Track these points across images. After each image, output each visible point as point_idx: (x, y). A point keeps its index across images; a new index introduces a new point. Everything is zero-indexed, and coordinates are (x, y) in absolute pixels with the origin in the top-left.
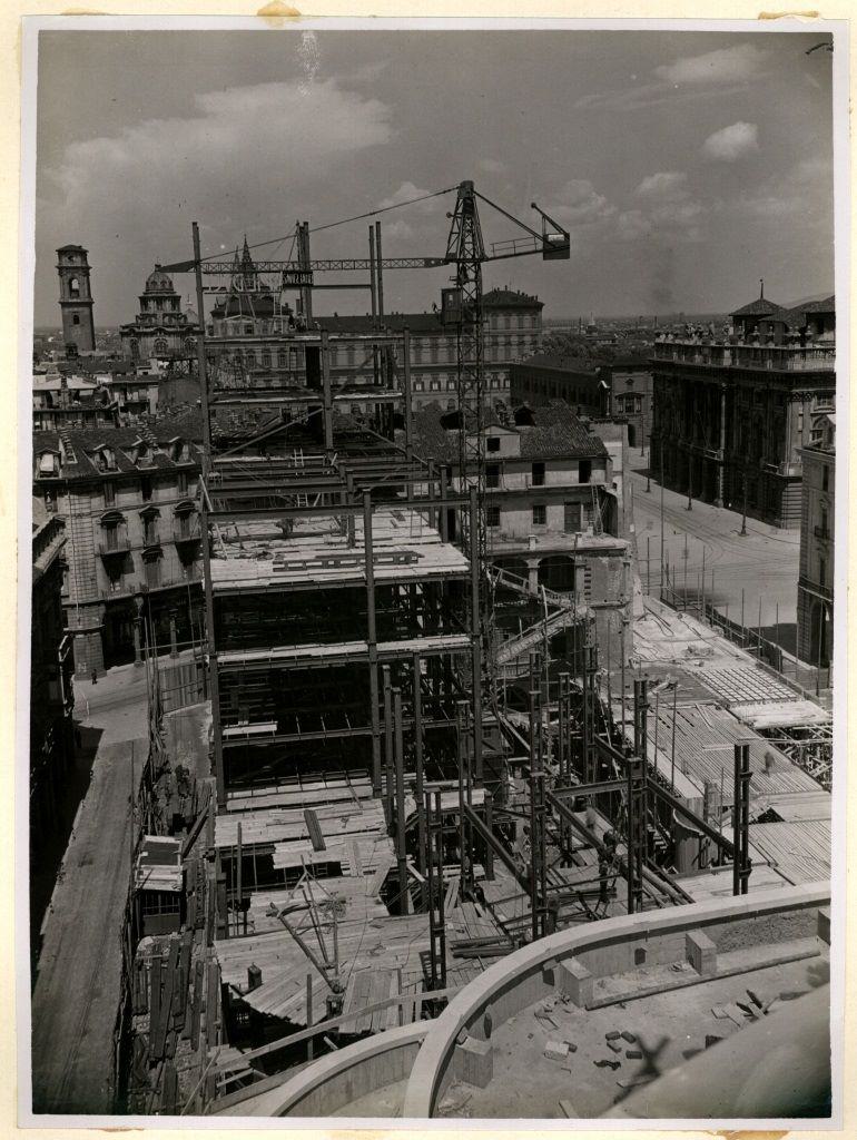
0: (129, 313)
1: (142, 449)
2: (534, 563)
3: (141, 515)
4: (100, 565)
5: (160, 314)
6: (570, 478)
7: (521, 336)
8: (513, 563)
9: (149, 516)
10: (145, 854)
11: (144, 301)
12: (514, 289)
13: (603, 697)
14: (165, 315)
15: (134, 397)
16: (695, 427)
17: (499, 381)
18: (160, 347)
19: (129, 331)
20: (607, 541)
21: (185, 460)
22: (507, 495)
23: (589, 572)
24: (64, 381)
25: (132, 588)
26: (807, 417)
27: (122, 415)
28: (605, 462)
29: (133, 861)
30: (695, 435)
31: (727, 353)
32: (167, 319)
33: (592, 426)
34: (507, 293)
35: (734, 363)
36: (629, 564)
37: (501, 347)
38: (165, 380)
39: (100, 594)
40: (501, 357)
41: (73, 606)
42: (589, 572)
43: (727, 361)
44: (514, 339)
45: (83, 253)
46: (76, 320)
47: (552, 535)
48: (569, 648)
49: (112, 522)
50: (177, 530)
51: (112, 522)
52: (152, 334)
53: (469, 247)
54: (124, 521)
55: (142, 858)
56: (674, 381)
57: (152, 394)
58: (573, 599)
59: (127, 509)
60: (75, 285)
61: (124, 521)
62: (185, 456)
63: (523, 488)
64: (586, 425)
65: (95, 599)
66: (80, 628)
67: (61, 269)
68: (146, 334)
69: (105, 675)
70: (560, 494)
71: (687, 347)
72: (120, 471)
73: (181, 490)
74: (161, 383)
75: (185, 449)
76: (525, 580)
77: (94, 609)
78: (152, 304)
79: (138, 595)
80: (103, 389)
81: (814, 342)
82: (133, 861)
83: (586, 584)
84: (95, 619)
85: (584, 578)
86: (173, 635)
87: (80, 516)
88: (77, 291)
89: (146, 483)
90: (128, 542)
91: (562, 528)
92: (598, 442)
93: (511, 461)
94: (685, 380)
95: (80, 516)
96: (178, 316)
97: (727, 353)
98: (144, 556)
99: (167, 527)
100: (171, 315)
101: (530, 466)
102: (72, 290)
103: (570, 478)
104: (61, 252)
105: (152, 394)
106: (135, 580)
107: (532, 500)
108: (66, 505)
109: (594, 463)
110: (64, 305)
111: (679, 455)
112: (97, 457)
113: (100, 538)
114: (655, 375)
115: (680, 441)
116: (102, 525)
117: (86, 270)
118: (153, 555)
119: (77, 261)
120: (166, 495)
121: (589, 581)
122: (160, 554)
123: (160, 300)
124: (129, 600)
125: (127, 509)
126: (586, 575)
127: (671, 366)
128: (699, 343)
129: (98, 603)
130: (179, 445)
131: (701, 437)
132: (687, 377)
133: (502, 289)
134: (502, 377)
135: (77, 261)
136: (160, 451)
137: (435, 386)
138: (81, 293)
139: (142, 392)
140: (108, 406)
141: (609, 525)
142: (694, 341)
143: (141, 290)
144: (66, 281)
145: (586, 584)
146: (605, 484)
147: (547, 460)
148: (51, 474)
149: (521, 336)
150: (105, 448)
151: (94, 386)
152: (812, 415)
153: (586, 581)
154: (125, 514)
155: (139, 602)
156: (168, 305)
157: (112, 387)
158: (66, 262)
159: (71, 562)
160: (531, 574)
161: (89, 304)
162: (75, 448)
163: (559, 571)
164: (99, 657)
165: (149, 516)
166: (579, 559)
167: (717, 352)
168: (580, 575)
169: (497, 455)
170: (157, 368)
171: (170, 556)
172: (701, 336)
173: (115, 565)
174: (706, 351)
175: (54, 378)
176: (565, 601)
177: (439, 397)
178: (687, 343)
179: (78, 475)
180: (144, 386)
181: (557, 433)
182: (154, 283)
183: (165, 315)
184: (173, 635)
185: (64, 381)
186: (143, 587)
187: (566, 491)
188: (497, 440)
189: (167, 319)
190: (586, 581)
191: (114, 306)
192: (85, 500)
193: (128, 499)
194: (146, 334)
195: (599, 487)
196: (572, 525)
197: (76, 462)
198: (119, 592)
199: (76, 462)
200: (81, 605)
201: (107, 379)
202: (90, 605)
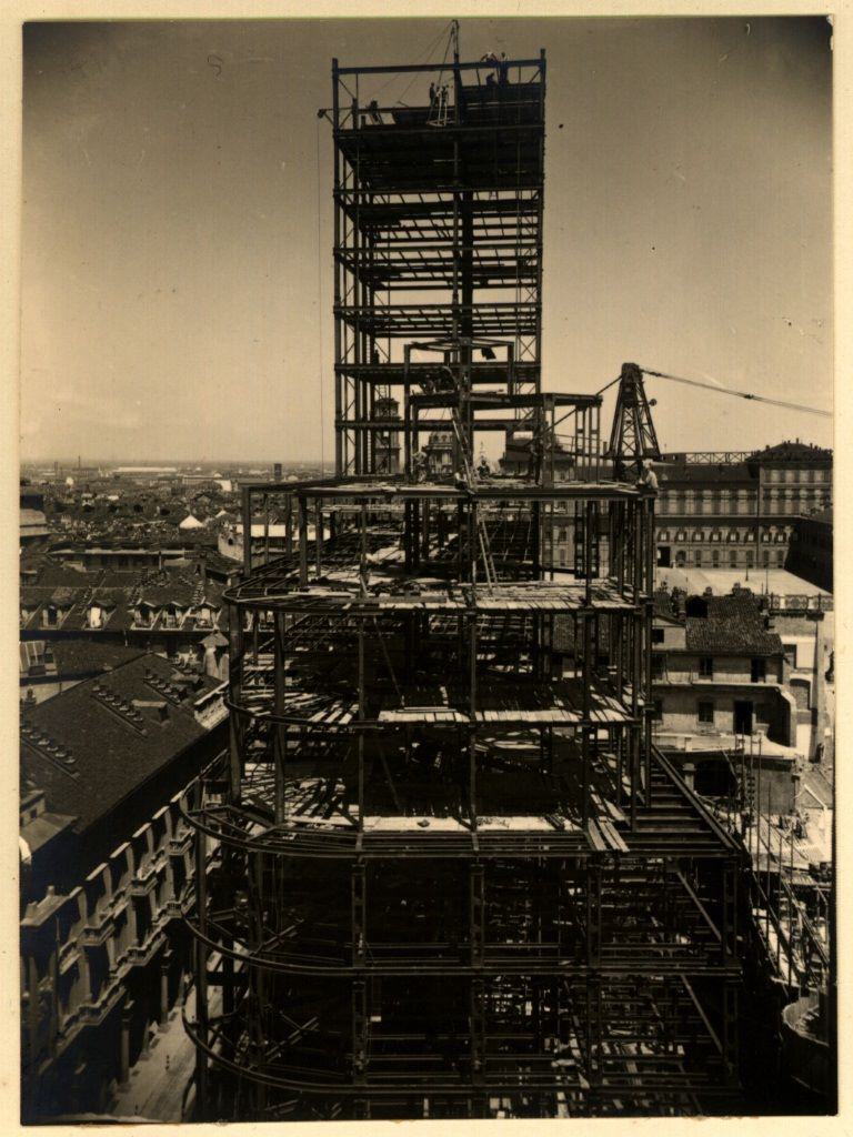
5: (439, 466)
6: (742, 679)
7: (811, 490)
12: (806, 442)
17: (770, 534)
20: (772, 749)
22: (670, 689)
28: (781, 664)
33: (771, 622)
34: (799, 446)
36: (798, 778)
37: (788, 501)
40: (788, 510)
44: (803, 493)
47: (720, 736)
53: (629, 440)
63: (686, 683)
64: (766, 620)
70: (724, 692)
91: (731, 729)
92: (776, 638)
93: (675, 653)
101: (695, 662)
103: (742, 679)
109: (769, 665)
133: (793, 441)
134: (788, 531)
137: (715, 537)
141: (782, 735)
146: (780, 686)
149: (811, 490)
163: (718, 774)
169: (660, 646)
177: (720, 549)
181: (732, 628)
183: (444, 466)
195: (773, 689)
196: (742, 726)
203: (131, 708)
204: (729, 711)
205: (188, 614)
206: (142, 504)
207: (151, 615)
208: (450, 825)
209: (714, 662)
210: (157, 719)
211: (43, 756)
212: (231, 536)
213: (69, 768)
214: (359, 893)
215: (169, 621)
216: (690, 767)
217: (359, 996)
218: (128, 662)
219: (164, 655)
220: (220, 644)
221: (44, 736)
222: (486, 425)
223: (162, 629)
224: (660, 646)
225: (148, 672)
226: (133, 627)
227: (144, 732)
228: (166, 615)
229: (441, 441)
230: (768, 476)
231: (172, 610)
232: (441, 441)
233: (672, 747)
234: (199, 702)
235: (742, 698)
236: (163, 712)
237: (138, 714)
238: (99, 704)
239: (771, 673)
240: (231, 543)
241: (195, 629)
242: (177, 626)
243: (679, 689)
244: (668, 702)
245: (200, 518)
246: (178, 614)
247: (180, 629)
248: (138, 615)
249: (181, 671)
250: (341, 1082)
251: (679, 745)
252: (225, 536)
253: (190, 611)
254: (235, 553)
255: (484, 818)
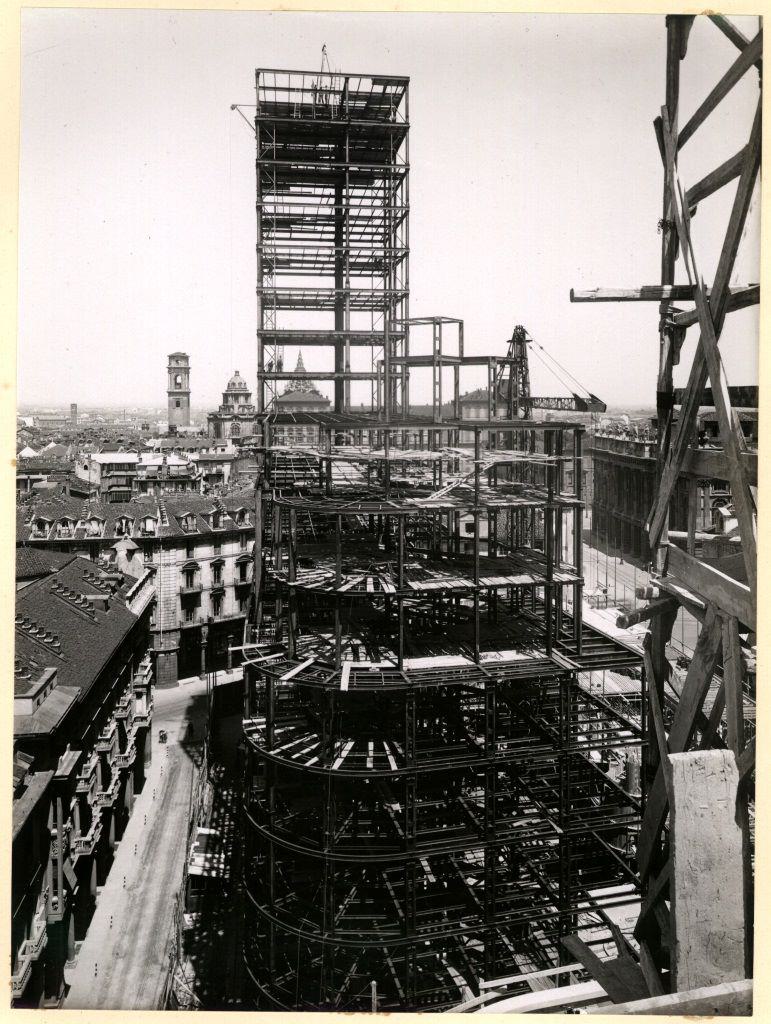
0: (215, 403)
1: (217, 515)
3: (211, 565)
4: (179, 602)
5: (236, 406)
9: (217, 566)
10: (197, 844)
11: (226, 396)
14: (240, 406)
15: (214, 471)
16: (625, 500)
18: (235, 430)
19: (215, 419)
21: (247, 525)
24: (165, 459)
25: (201, 620)
26: (707, 498)
27: (203, 483)
29: (188, 850)
30: (625, 505)
31: (647, 449)
32: (241, 409)
35: (651, 455)
38: (236, 459)
39: (178, 624)
41: (158, 633)
43: (647, 455)
45: (185, 358)
46: (178, 404)
49: (190, 571)
50: (238, 577)
51: (190, 571)
52: (230, 420)
54: (198, 569)
55: (195, 847)
56: (610, 464)
57: (226, 469)
59: (203, 560)
60: (179, 380)
61: (198, 569)
62: (247, 522)
65: (173, 627)
66: (162, 649)
67: (170, 369)
68: (225, 420)
69: (178, 685)
71: (618, 441)
72: (199, 532)
73: (242, 546)
74: (233, 461)
75: (247, 516)
77: (173, 634)
78: (230, 399)
79: (205, 625)
80: (192, 465)
81: (710, 443)
82: (188, 850)
84: (173, 643)
86: (230, 658)
87: (168, 565)
88: (180, 384)
89: (216, 540)
90: (201, 586)
94: (616, 466)
95: (168, 565)
96: (249, 407)
97: (647, 449)
98: (211, 595)
99: (230, 574)
100: (244, 407)
102: (176, 384)
104: (171, 357)
105: (226, 469)
106: (204, 610)
108: (160, 557)
110: (170, 394)
111: (614, 521)
112: (184, 523)
113: (181, 581)
114: (595, 460)
115: (614, 511)
116: (183, 572)
117: (187, 370)
118: (217, 597)
119: (182, 364)
120: (231, 549)
122: (224, 593)
123: (236, 396)
124: (199, 628)
125: (203, 560)
127: (607, 454)
128: (627, 439)
129: (175, 630)
130: (242, 514)
131: (630, 508)
132: (619, 463)
135: (182, 364)
136: (228, 518)
138: (183, 386)
139: (219, 467)
140: (193, 478)
142: (623, 437)
143: (224, 389)
144: (173, 377)
148: (152, 533)
150: (188, 516)
151: (185, 463)
152: (711, 497)
154: (200, 564)
155: (205, 630)
156: (242, 400)
157: (198, 462)
158: (174, 364)
159: (161, 599)
161: (187, 394)
162: (169, 514)
164: (175, 671)
165: (217, 566)
167: (640, 447)
170: (231, 450)
171: (230, 593)
172: (627, 435)
173: (190, 602)
174: (632, 445)
175: (158, 457)
178: (618, 438)
179: (169, 535)
180: (221, 462)
182: (234, 384)
183: (240, 406)
184: (230, 658)
185: (165, 459)
186: (210, 619)
189: (241, 409)
191: (206, 396)
192: (173, 551)
193: (203, 552)
194: (225, 420)
197: (168, 525)
198: (190, 625)
199: (168, 525)
200: (164, 632)
201: (195, 456)
202: (170, 631)
203: (85, 600)
205: (79, 525)
206: (122, 438)
207: (47, 527)
208: (459, 661)
210: (101, 609)
211: (33, 641)
212: (86, 463)
213: (57, 650)
214: (411, 715)
215: (63, 532)
217: (411, 788)
218: (66, 565)
219: (88, 557)
220: (132, 548)
221: (34, 625)
222: (363, 376)
223: (57, 538)
225: (86, 572)
226: (31, 538)
227: (96, 619)
228: (59, 527)
229: (237, 386)
230: (468, 414)
231: (65, 523)
232: (237, 386)
234: (129, 594)
236: (106, 605)
237: (91, 604)
238: (59, 599)
240: (86, 468)
241: (85, 538)
242: (70, 536)
245: (35, 448)
246: (71, 526)
247: (73, 538)
248: (35, 528)
249: (105, 570)
250: (399, 852)
252: (81, 463)
253: (79, 522)
254: (92, 476)
255: (485, 653)
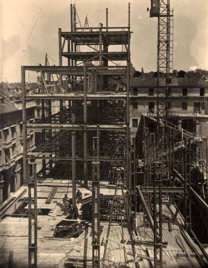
2: (180, 121)
8: (174, 120)
13: (201, 171)
23: (201, 126)
42: (201, 126)
47: (189, 113)
48: (191, 151)
58: (195, 135)
76: (176, 126)
83: (200, 130)
85: (199, 128)
93: (175, 87)
101: (182, 89)
107: (182, 101)
121: (201, 129)
126: (200, 127)
145: (200, 130)
147: (188, 87)
153: (200, 129)
160: (179, 125)
163: (190, 124)
166: (197, 122)
168: (198, 127)
169: (170, 85)
176: (189, 134)
181: (193, 80)
187: (195, 98)
188: (170, 80)
190: (200, 129)
204: (193, 106)
209: (188, 89)
216: (180, 121)
224: (170, 85)
233: (175, 116)
235: (197, 101)
239: (190, 106)
243: (176, 98)
244: (173, 103)
251: (177, 114)
